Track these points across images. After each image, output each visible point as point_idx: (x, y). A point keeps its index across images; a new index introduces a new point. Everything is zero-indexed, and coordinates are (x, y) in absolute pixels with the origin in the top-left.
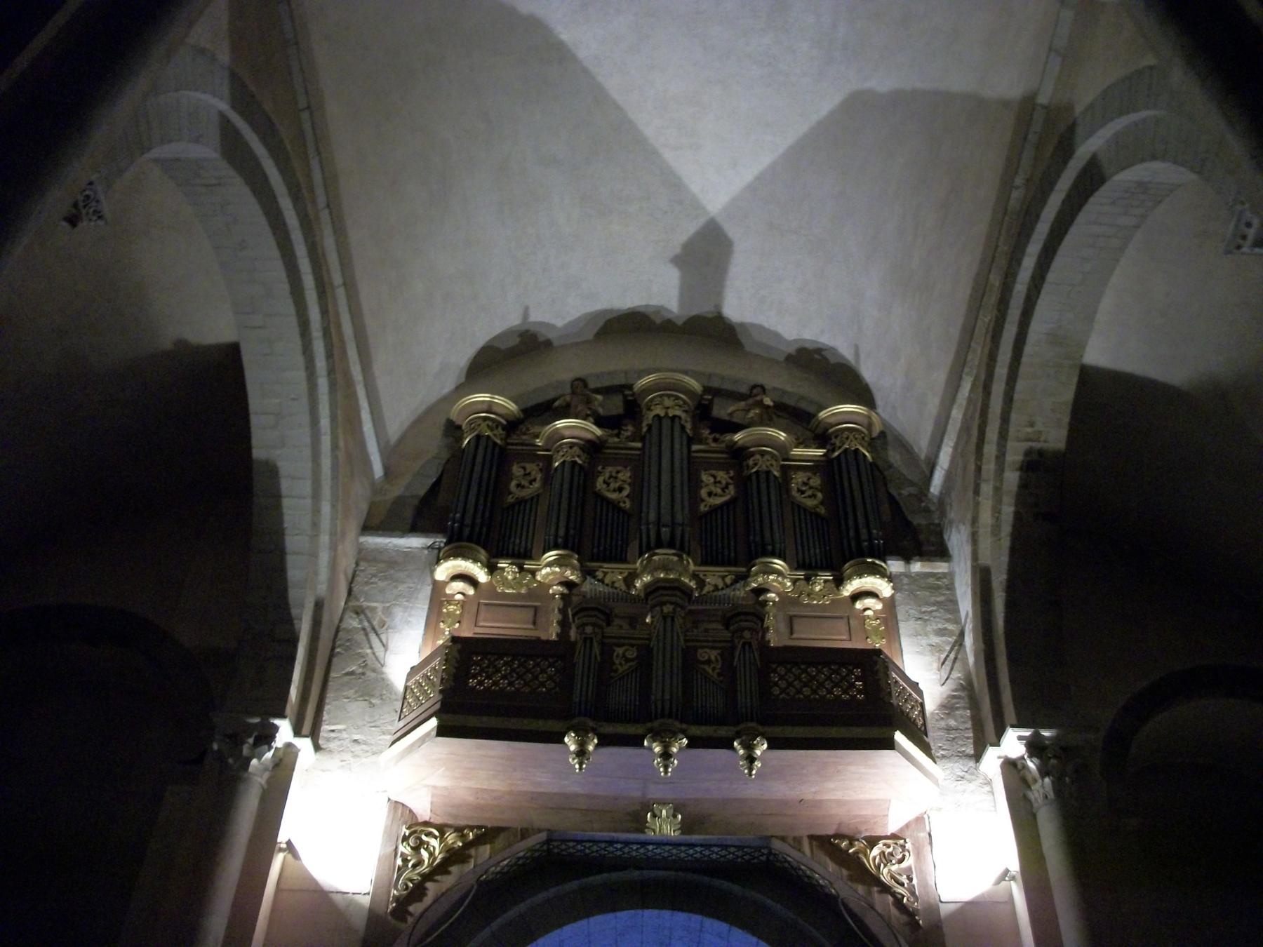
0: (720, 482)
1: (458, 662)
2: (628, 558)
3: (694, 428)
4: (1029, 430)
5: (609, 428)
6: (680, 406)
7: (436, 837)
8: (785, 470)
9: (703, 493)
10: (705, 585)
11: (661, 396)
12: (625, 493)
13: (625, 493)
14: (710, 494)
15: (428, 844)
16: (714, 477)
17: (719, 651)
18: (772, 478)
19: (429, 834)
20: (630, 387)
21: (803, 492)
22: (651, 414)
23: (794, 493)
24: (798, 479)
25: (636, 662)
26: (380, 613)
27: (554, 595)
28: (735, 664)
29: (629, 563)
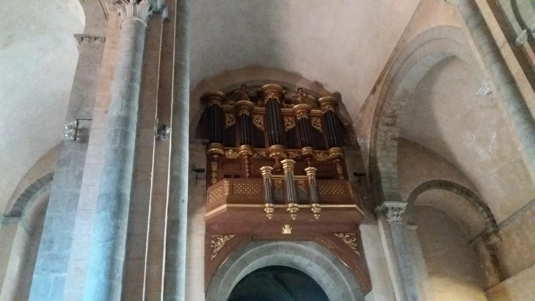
0: (290, 121)
1: (229, 186)
2: (266, 147)
3: (281, 102)
4: (393, 114)
5: (254, 102)
6: (276, 95)
7: (221, 238)
8: (309, 117)
9: (286, 124)
10: (290, 155)
11: (270, 91)
12: (262, 125)
13: (262, 125)
14: (288, 125)
15: (220, 240)
16: (288, 119)
17: (304, 181)
18: (306, 119)
19: (219, 237)
20: (260, 86)
21: (315, 125)
22: (268, 98)
23: (313, 125)
24: (314, 119)
25: (281, 185)
26: (348, 243)
27: (245, 159)
28: (309, 186)
29: (266, 148)
